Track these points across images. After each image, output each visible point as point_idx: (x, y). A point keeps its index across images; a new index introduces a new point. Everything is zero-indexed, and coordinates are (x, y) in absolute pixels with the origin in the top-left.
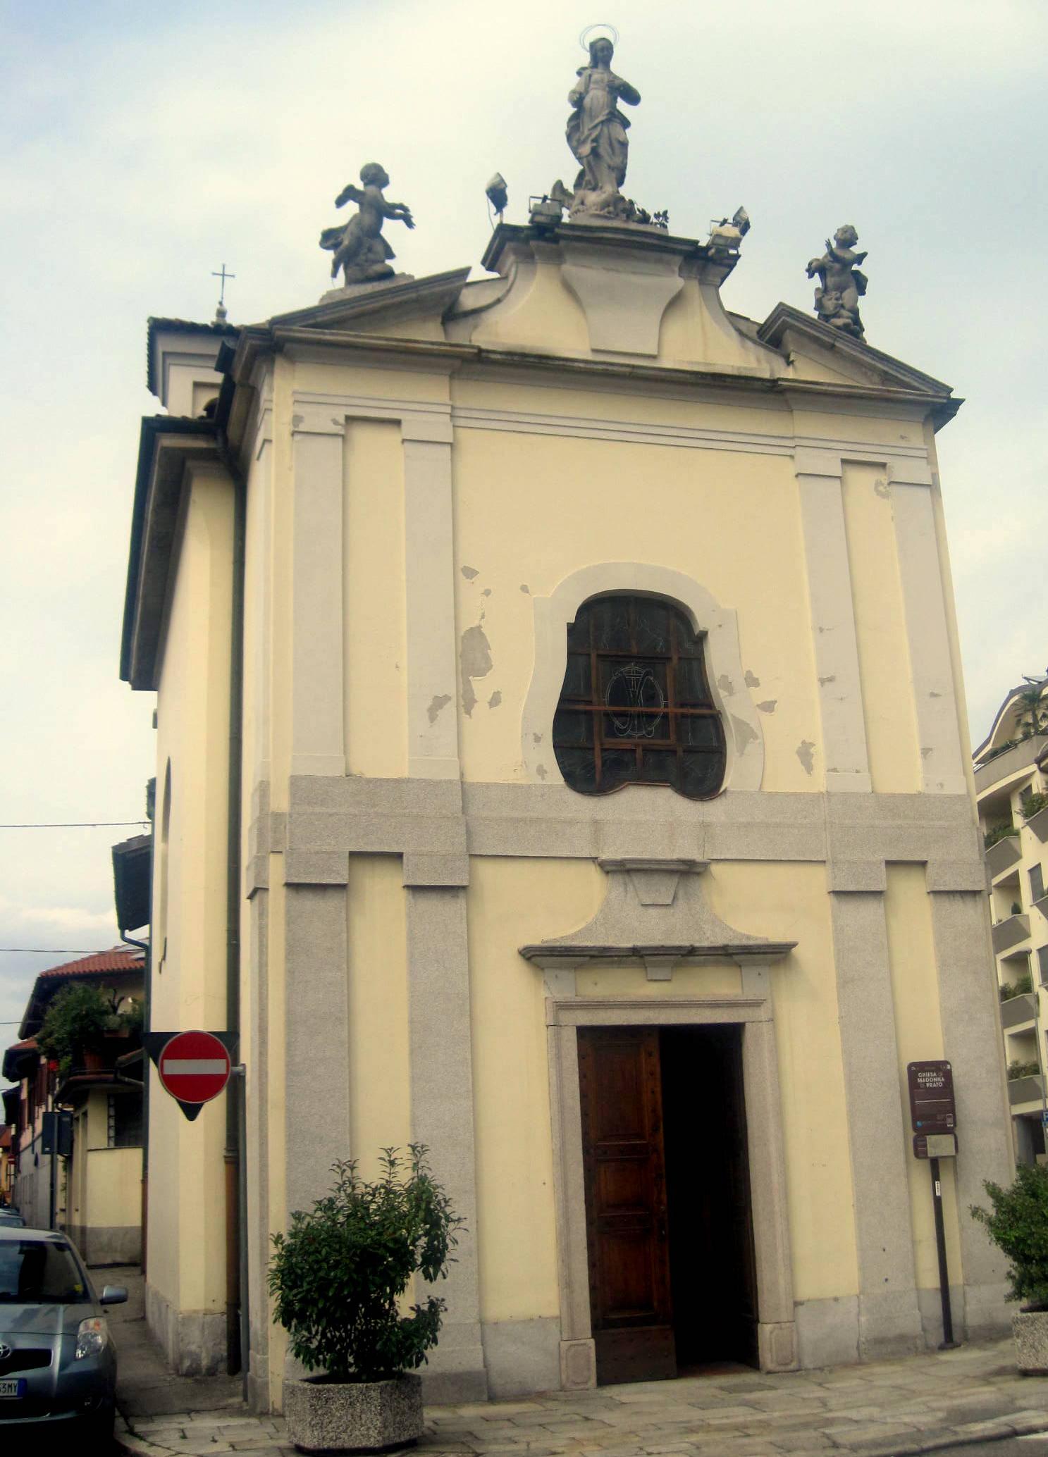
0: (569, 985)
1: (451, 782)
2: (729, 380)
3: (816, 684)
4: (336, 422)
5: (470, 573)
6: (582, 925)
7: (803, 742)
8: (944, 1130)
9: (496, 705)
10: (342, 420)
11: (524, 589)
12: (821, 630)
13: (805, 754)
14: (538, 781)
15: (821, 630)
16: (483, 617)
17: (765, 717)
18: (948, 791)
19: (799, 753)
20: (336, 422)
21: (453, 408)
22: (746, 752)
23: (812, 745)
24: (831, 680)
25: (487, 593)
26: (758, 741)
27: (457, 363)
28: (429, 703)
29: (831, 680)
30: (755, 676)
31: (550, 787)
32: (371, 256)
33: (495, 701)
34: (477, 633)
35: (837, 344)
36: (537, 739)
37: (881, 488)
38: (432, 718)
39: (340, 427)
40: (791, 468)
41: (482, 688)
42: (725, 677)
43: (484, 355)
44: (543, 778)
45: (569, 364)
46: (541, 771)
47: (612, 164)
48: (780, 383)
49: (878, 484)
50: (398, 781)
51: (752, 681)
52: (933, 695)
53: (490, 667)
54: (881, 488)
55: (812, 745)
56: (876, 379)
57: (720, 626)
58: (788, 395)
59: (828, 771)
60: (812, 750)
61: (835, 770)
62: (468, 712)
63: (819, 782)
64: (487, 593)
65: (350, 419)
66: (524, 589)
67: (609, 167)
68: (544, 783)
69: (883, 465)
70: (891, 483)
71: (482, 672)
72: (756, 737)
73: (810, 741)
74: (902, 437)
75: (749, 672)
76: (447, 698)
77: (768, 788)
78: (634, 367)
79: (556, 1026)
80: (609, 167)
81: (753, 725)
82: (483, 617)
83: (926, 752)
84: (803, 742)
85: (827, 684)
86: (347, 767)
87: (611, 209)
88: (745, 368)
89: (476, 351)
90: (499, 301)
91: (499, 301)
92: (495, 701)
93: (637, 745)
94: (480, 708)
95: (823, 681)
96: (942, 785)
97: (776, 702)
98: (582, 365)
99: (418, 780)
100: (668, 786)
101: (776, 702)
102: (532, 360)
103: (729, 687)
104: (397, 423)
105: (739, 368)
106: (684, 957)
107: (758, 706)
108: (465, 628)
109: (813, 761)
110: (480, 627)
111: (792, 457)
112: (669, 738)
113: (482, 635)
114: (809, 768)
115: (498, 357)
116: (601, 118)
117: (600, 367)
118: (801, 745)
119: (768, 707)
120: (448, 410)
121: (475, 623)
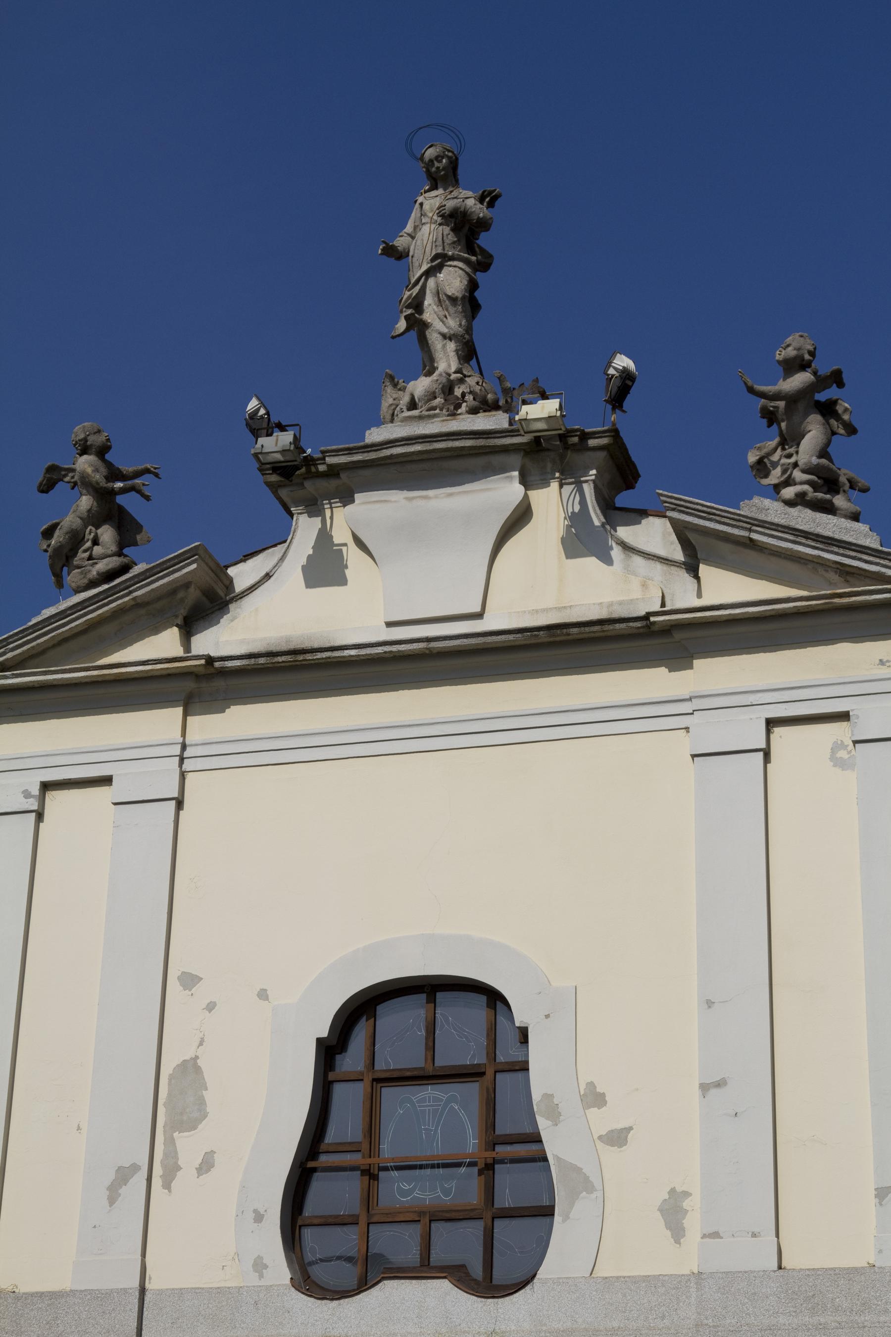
1: (125, 1291)
2: (575, 630)
3: (697, 1091)
4: (27, 795)
5: (190, 981)
7: (672, 1191)
9: (208, 1170)
10: (35, 790)
11: (263, 995)
12: (710, 1004)
14: (253, 1280)
15: (710, 1004)
16: (201, 1043)
17: (609, 1154)
20: (27, 795)
21: (184, 747)
22: (571, 1216)
23: (686, 1194)
24: (720, 1084)
26: (593, 1196)
27: (190, 685)
28: (111, 1176)
29: (720, 1084)
30: (599, 1090)
31: (268, 1288)
32: (97, 550)
33: (206, 1165)
35: (754, 536)
36: (259, 1218)
37: (842, 754)
38: (112, 1200)
39: (31, 800)
40: (684, 745)
42: (548, 1097)
43: (217, 664)
44: (261, 1276)
45: (309, 657)
46: (259, 1266)
47: (445, 330)
48: (652, 619)
49: (838, 746)
50: (54, 1296)
54: (842, 754)
55: (686, 1194)
56: (834, 577)
57: (547, 1016)
58: (678, 635)
59: (704, 1236)
60: (686, 1204)
61: (716, 1235)
62: (167, 1185)
65: (46, 787)
66: (263, 995)
67: (444, 336)
68: (262, 1283)
69: (844, 716)
70: (855, 742)
71: (192, 1125)
72: (588, 1186)
73: (684, 1188)
74: (882, 663)
75: (591, 1085)
76: (135, 1168)
77: (603, 1271)
78: (428, 640)
80: (444, 336)
81: (589, 1170)
82: (201, 1043)
84: (672, 1191)
85: (713, 1092)
87: (439, 401)
88: (621, 603)
89: (203, 662)
90: (268, 576)
91: (268, 576)
92: (206, 1165)
94: (186, 1177)
95: (705, 1088)
97: (631, 1128)
98: (353, 652)
99: (81, 1291)
100: (445, 1278)
101: (631, 1128)
102: (283, 658)
103: (555, 1115)
104: (107, 781)
105: (611, 604)
107: (600, 1138)
109: (686, 1222)
110: (197, 1057)
111: (687, 729)
113: (198, 1070)
114: (677, 1232)
115: (237, 663)
116: (425, 267)
117: (379, 650)
118: (667, 1197)
120: (177, 750)
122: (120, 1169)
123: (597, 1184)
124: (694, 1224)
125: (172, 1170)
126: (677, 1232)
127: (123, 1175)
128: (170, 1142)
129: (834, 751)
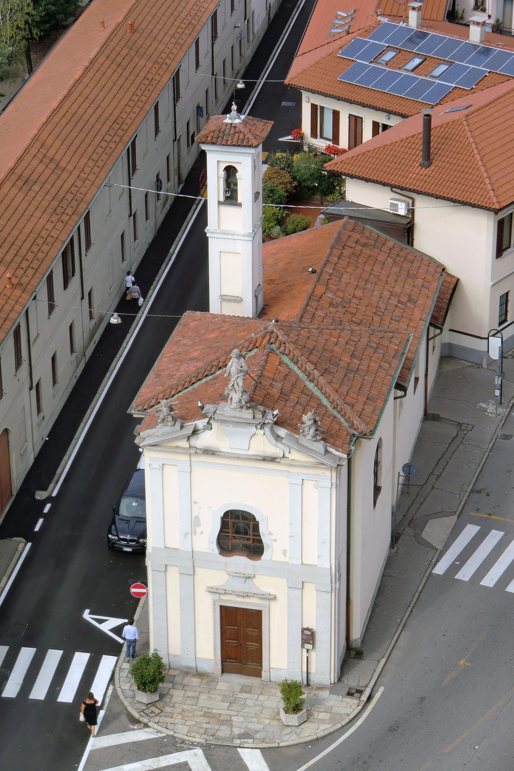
0: (217, 597)
5: (196, 503)
6: (222, 584)
8: (309, 643)
11: (210, 507)
12: (291, 524)
13: (284, 552)
15: (291, 524)
17: (273, 543)
18: (324, 566)
19: (282, 552)
23: (286, 550)
24: (293, 536)
25: (200, 508)
29: (293, 536)
33: (202, 533)
34: (197, 517)
37: (316, 486)
41: (198, 530)
46: (213, 550)
51: (270, 534)
52: (323, 543)
53: (200, 525)
55: (286, 550)
61: (291, 558)
62: (195, 535)
63: (287, 559)
64: (200, 508)
66: (210, 507)
72: (270, 547)
75: (270, 532)
76: (189, 533)
77: (273, 559)
79: (214, 605)
83: (319, 556)
86: (165, 545)
92: (202, 533)
93: (241, 543)
95: (290, 537)
96: (322, 565)
103: (264, 536)
106: (247, 595)
108: (194, 515)
112: (250, 541)
114: (285, 556)
119: (275, 540)
121: (197, 515)
122: (186, 533)
123: (271, 546)
124: (288, 555)
125: (195, 533)
126: (285, 556)
127: (186, 534)
128: (194, 528)
129: (314, 485)
